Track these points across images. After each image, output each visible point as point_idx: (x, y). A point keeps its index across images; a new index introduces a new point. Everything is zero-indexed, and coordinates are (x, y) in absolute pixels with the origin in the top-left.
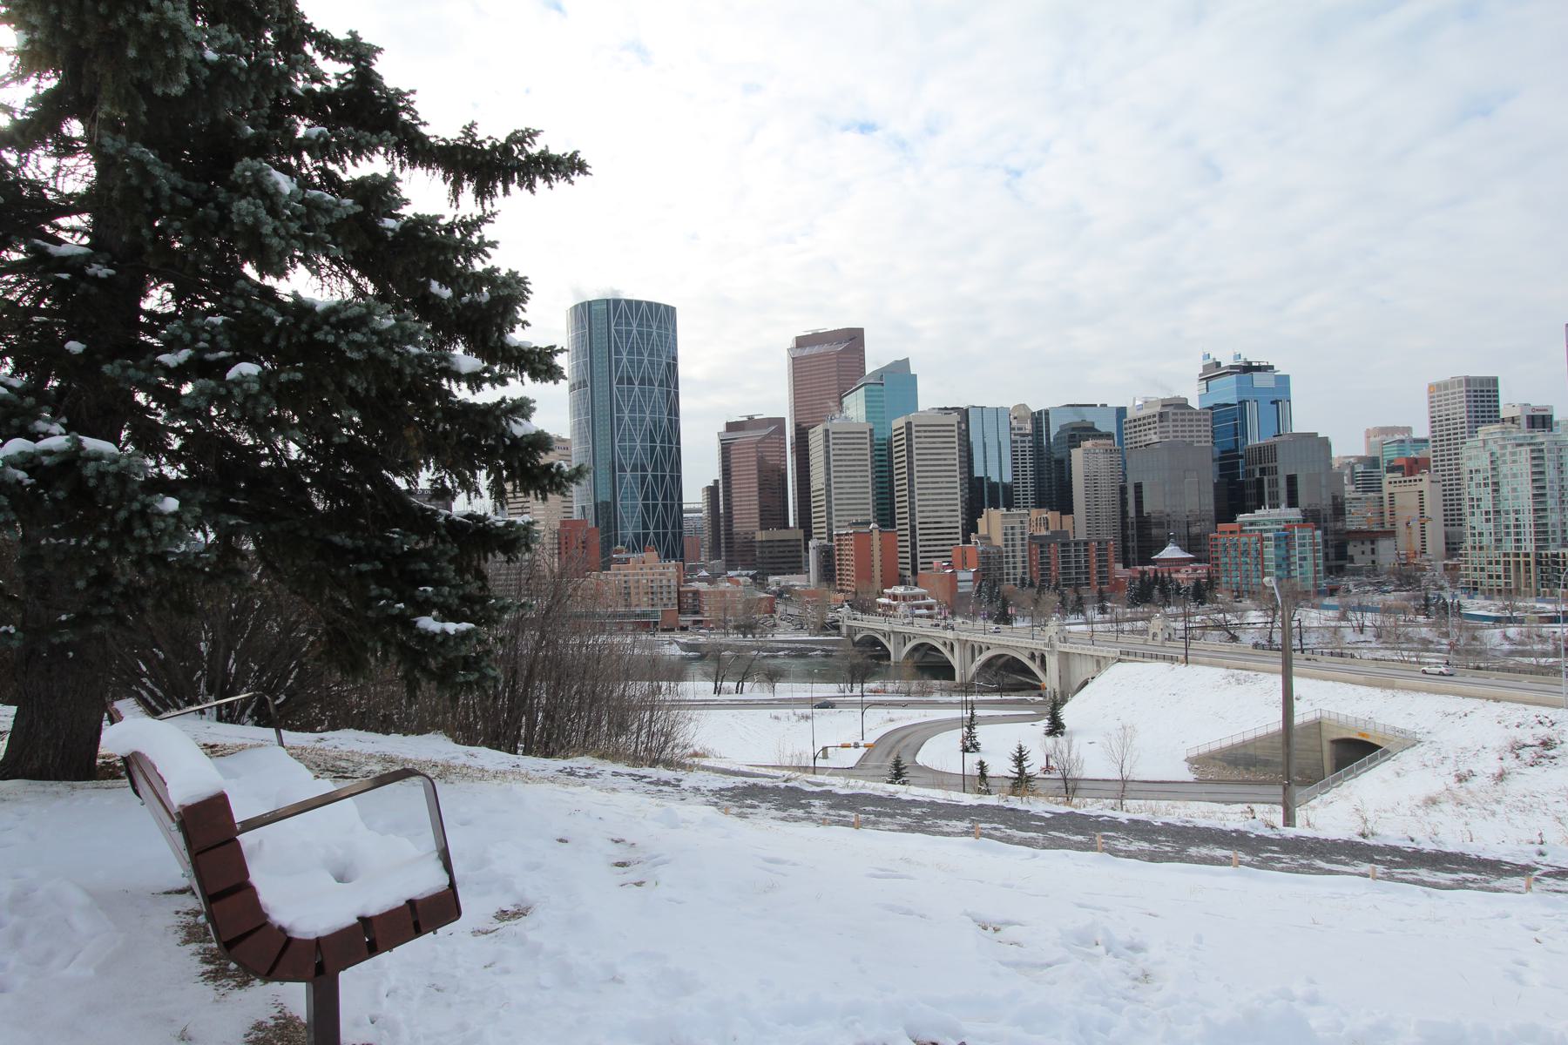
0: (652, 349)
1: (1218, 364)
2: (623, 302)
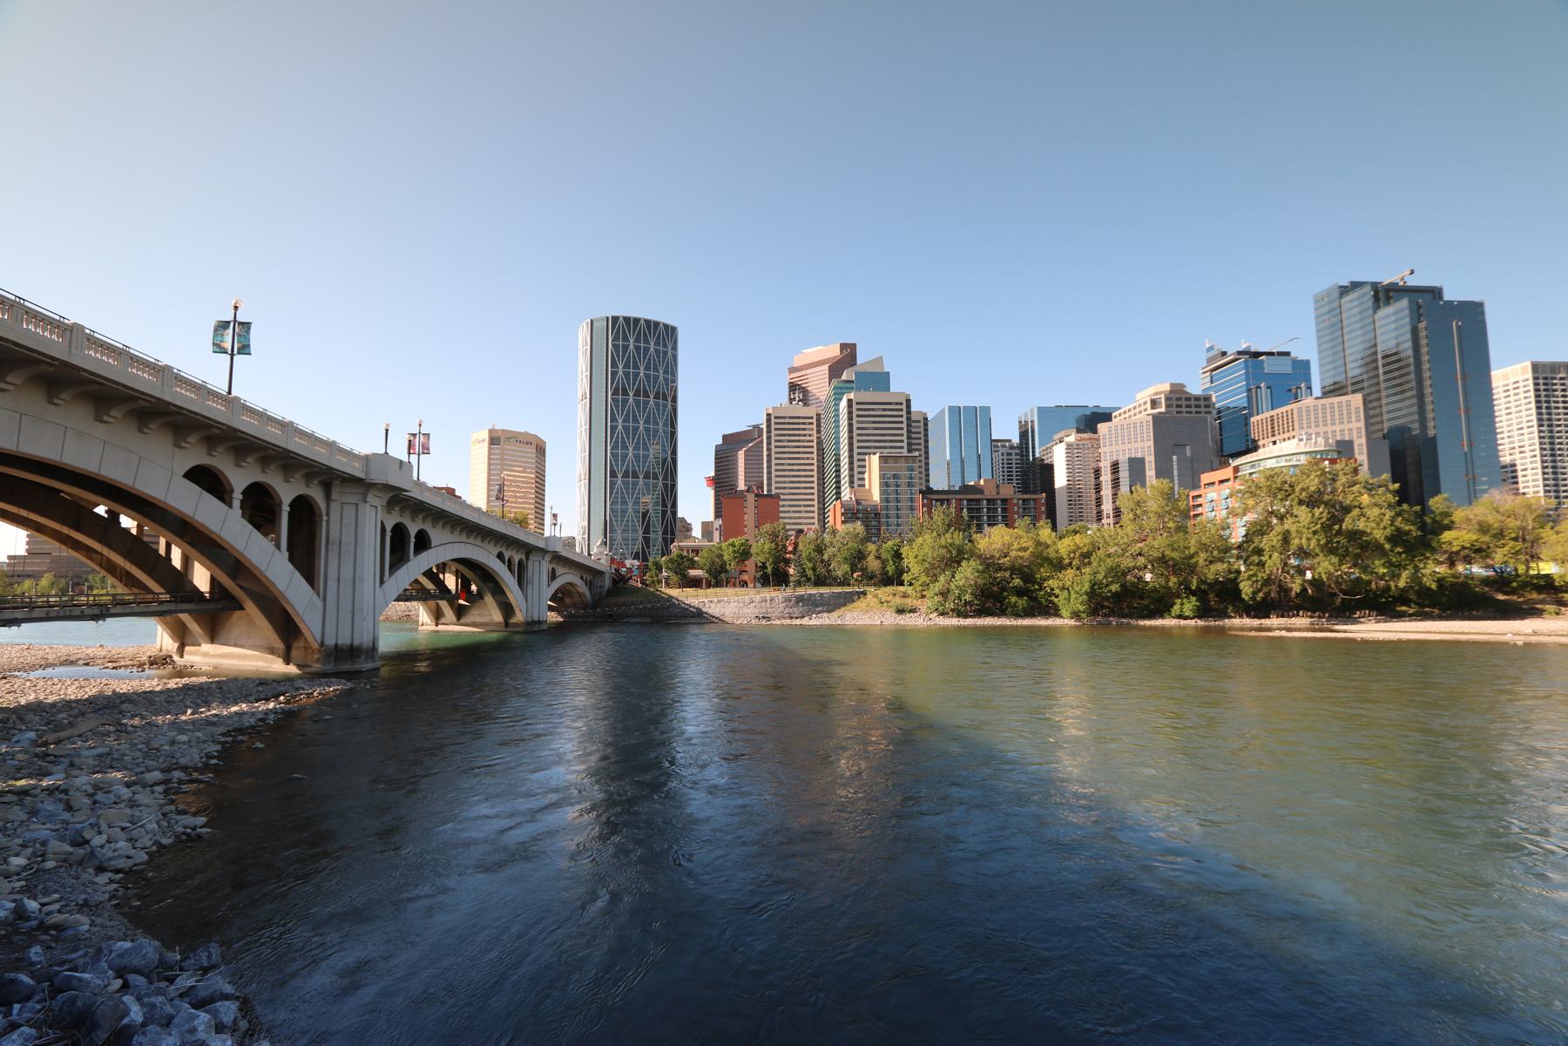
0: (649, 363)
1: (1224, 354)
2: (621, 319)
